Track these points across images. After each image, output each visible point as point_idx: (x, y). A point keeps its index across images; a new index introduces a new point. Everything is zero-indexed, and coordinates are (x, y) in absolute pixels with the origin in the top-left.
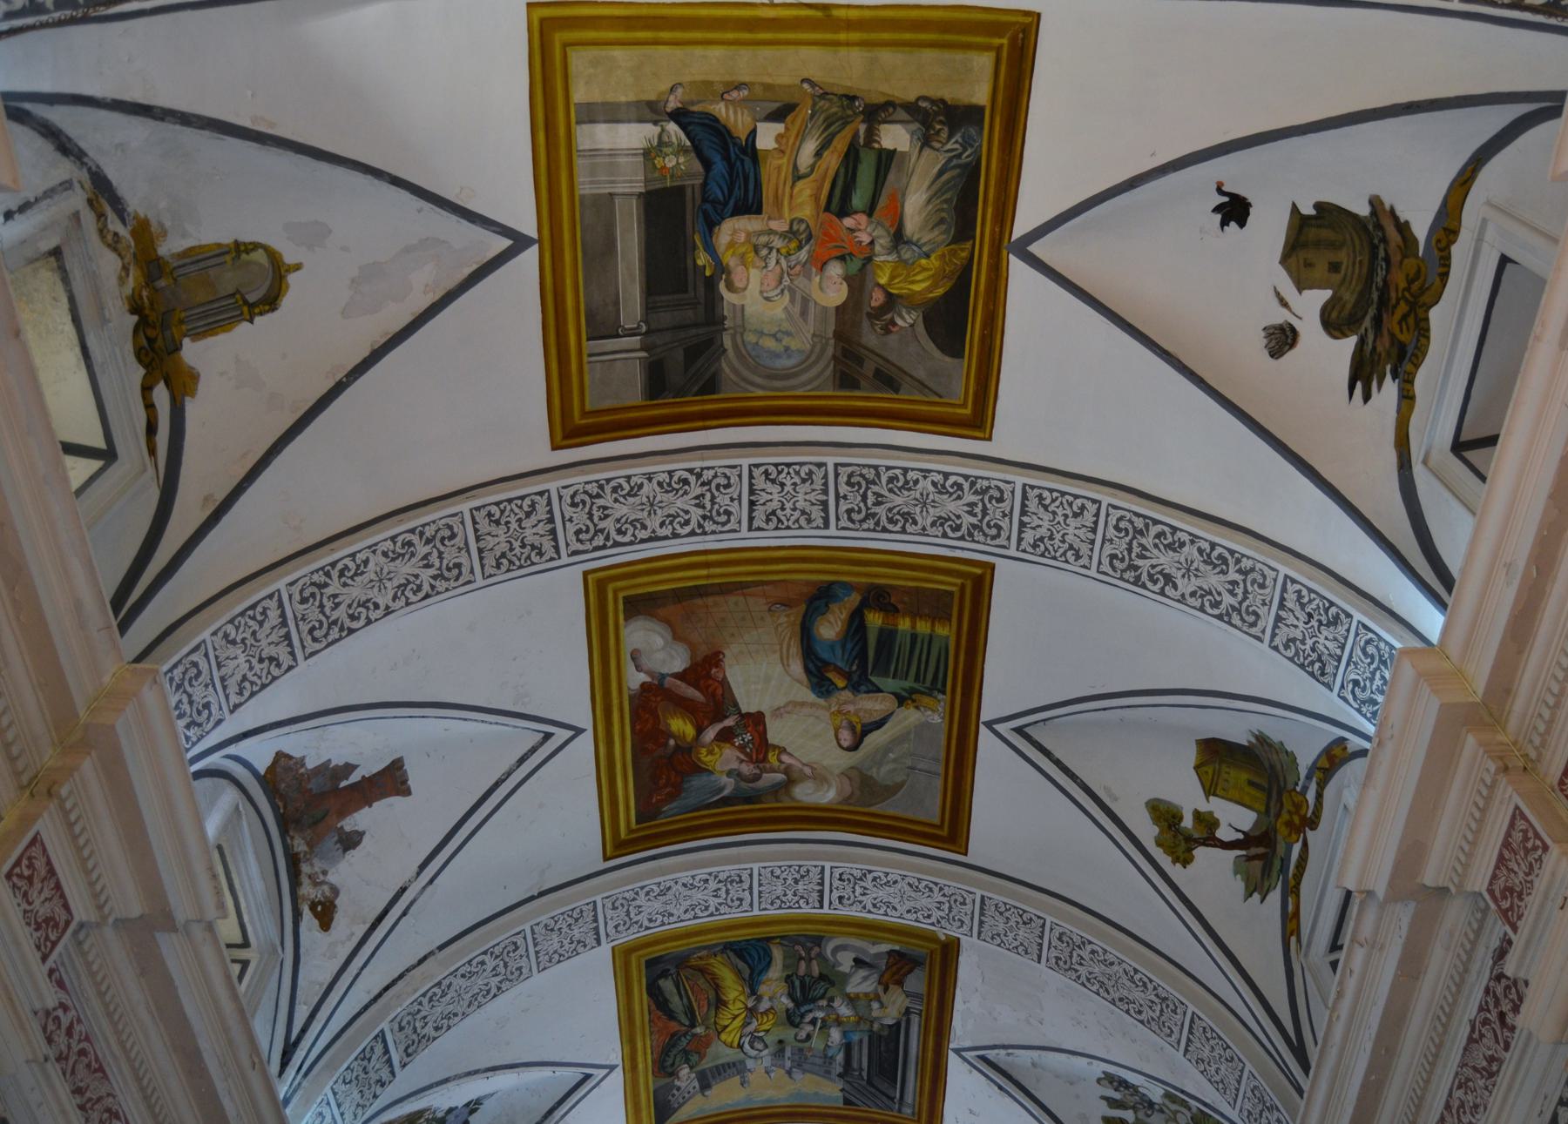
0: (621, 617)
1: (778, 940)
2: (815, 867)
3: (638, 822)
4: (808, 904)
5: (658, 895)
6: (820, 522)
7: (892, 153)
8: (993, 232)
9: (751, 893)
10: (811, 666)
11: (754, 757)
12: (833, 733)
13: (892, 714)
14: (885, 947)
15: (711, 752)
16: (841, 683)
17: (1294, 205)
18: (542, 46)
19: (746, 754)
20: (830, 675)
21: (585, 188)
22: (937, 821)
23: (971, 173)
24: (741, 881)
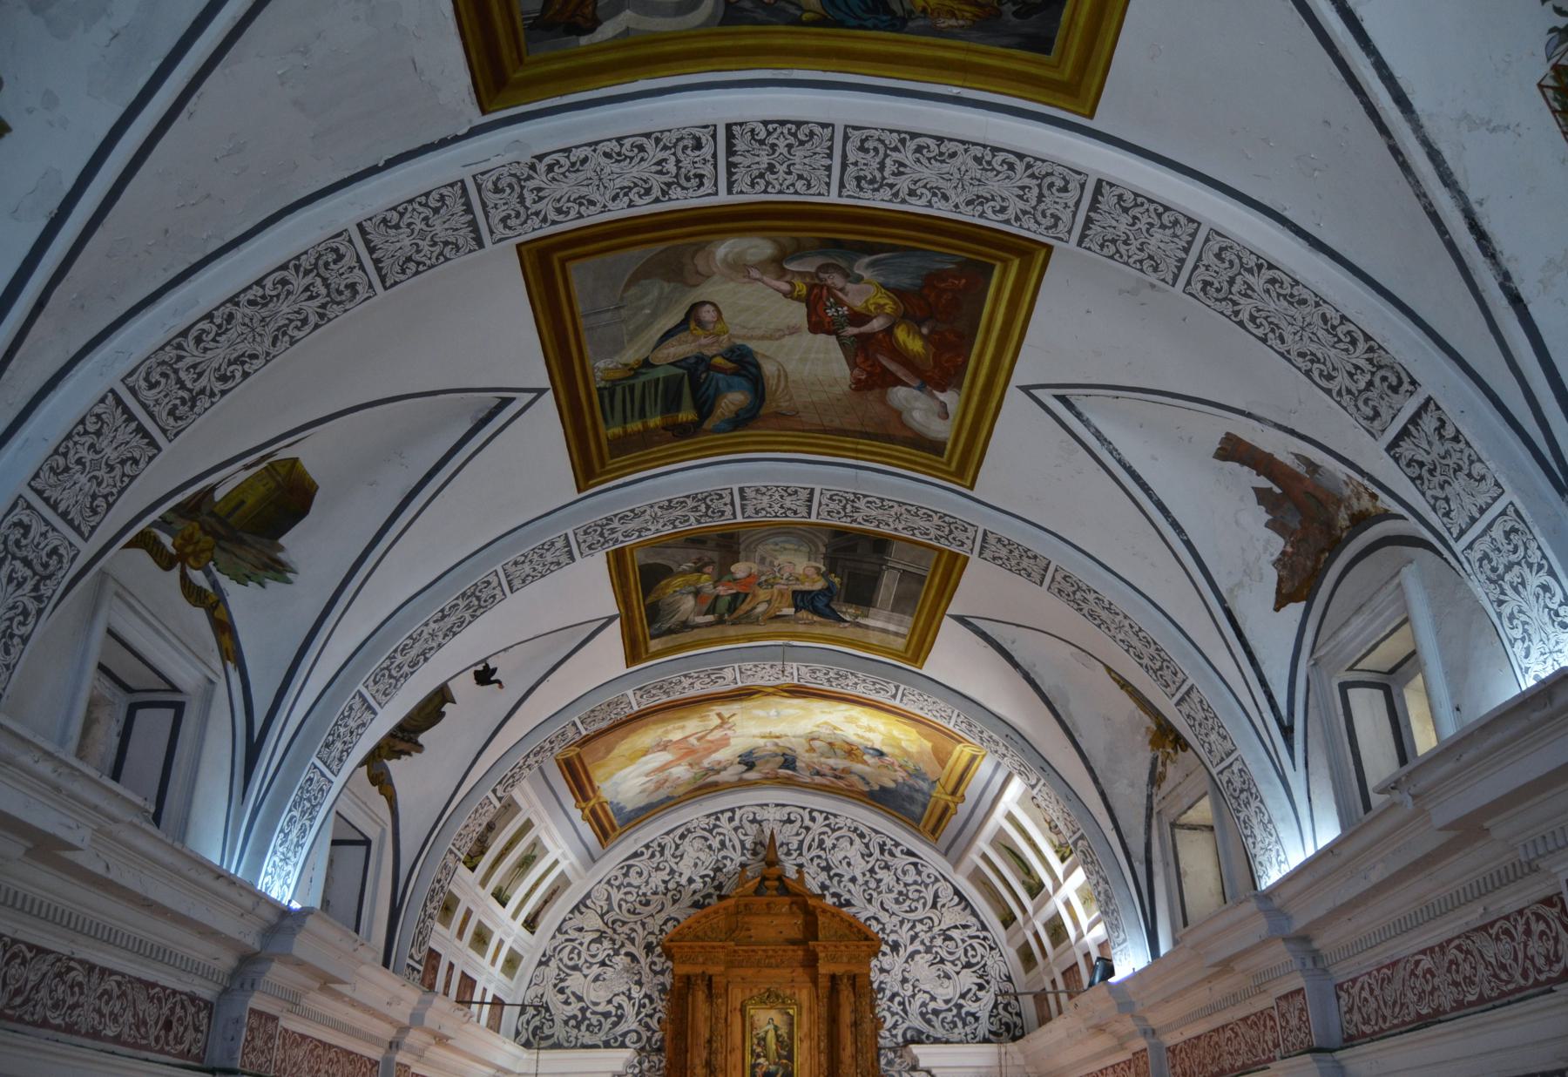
0: (949, 446)
1: (806, 16)
2: (742, 192)
3: (992, 267)
4: (753, 131)
5: (988, 200)
6: (747, 490)
7: (706, 614)
8: (633, 611)
9: (844, 156)
10: (753, 370)
11: (825, 291)
12: (725, 315)
13: (655, 349)
14: (607, 30)
15: (880, 307)
16: (718, 361)
17: (454, 702)
19: (835, 296)
20: (730, 365)
21: (909, 620)
22: (571, 266)
24: (858, 179)
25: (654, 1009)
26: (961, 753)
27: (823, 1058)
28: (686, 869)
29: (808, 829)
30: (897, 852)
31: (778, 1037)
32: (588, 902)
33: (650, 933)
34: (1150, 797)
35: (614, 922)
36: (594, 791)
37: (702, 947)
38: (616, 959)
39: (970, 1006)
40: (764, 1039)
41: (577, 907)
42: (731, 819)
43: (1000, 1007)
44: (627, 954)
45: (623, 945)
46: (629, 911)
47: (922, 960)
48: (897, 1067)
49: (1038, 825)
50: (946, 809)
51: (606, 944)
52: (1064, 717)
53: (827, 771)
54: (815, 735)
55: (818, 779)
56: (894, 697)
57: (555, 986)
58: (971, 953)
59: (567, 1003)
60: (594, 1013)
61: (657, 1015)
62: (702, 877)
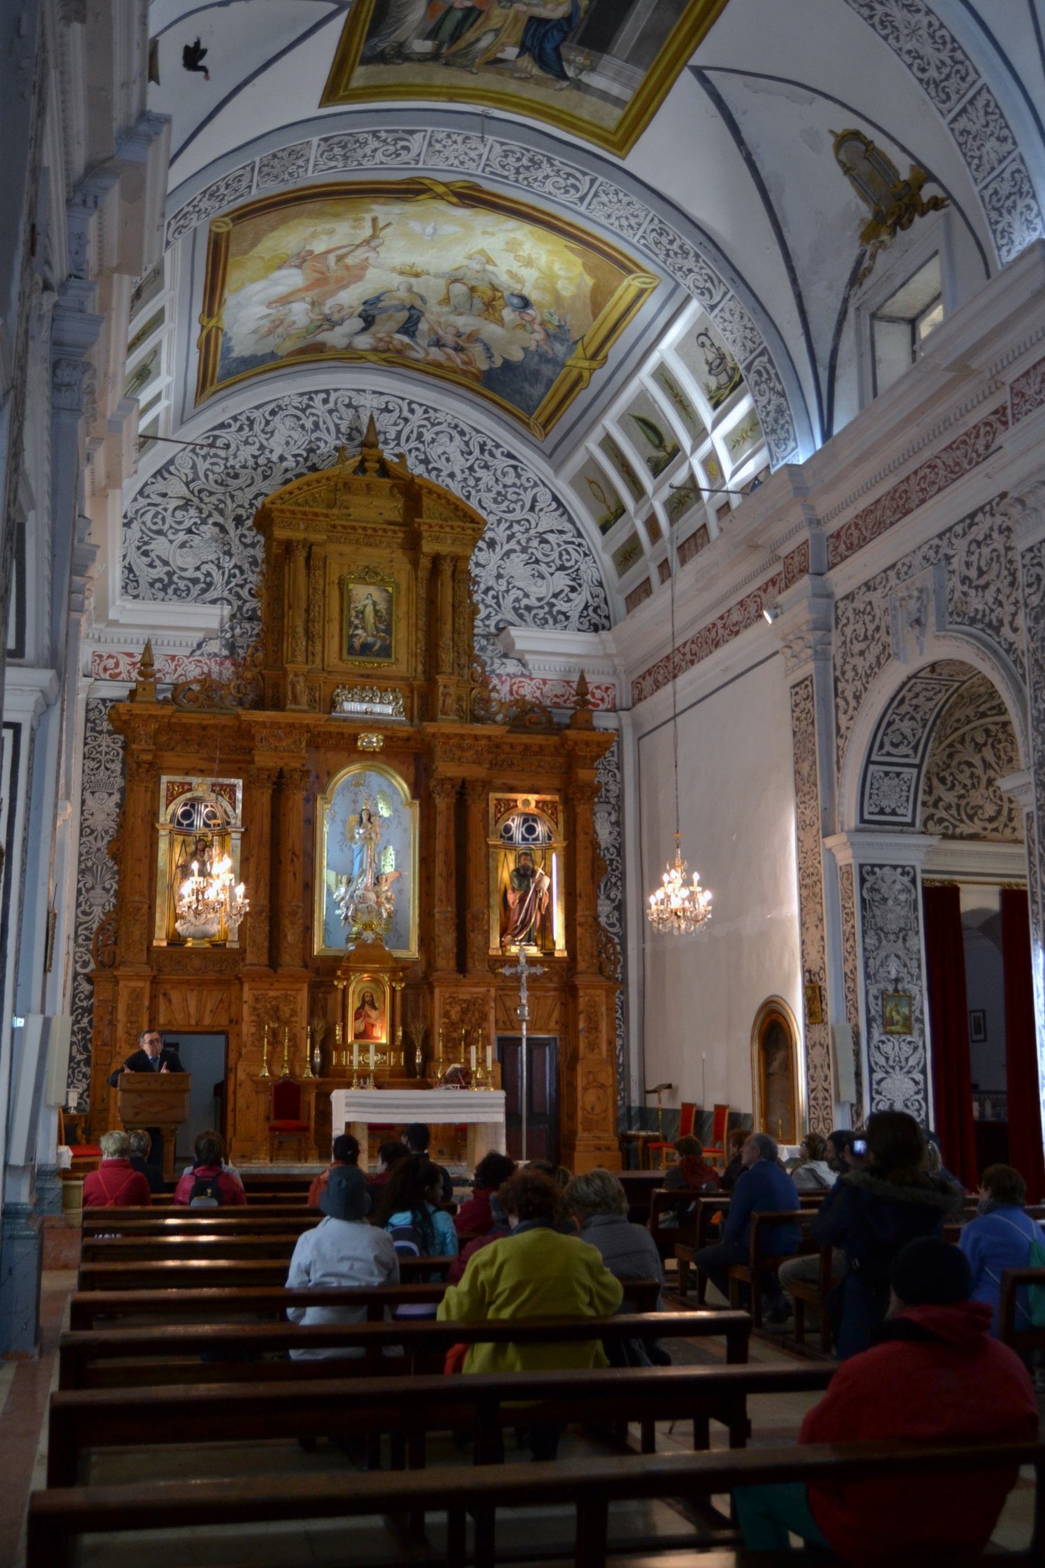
17: (158, 82)
18: (627, 141)
23: (374, 31)
25: (245, 580)
26: (631, 284)
27: (420, 635)
28: (277, 446)
29: (406, 420)
30: (498, 453)
31: (376, 612)
32: (172, 469)
33: (239, 506)
34: (846, 301)
35: (200, 491)
36: (220, 306)
37: (305, 513)
38: (203, 528)
39: (561, 605)
40: (362, 612)
41: (159, 472)
42: (325, 401)
43: (590, 609)
44: (215, 524)
45: (210, 515)
46: (216, 482)
47: (518, 559)
48: (489, 653)
49: (694, 371)
50: (579, 378)
51: (192, 512)
52: (776, 209)
53: (449, 339)
54: (459, 274)
55: (435, 353)
56: (582, 199)
57: (139, 548)
58: (565, 557)
59: (151, 565)
60: (181, 578)
61: (248, 587)
62: (295, 456)
